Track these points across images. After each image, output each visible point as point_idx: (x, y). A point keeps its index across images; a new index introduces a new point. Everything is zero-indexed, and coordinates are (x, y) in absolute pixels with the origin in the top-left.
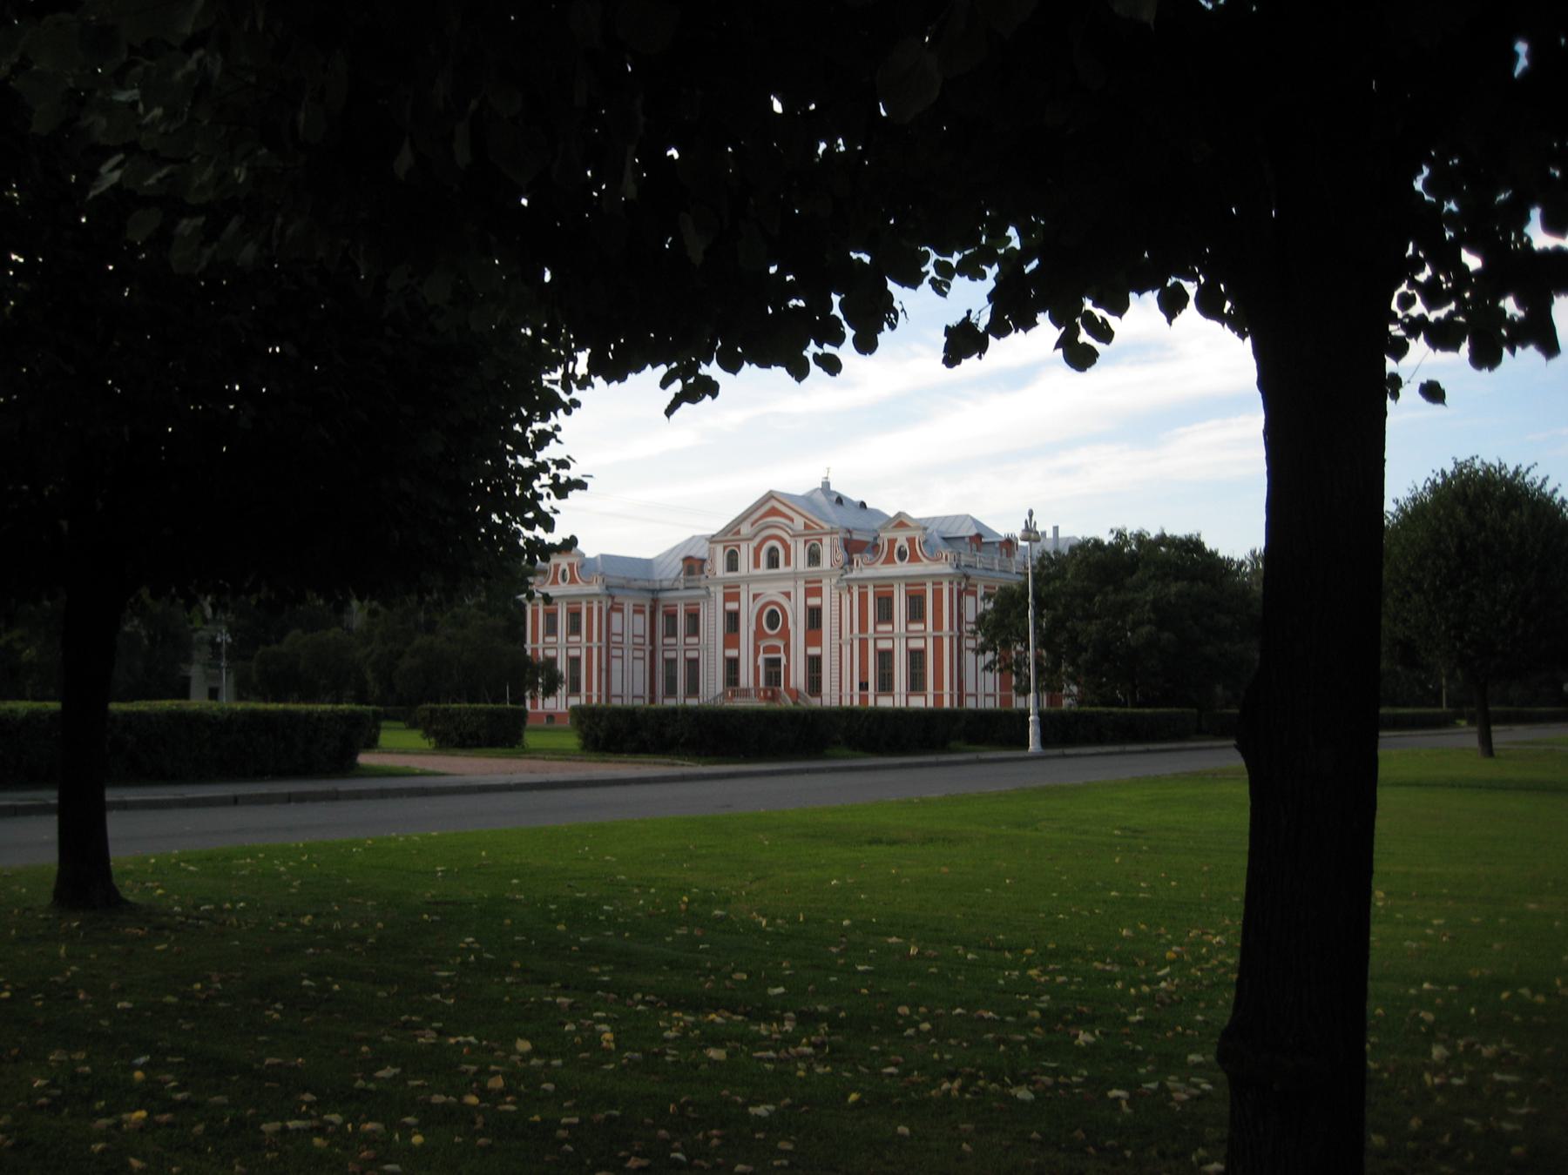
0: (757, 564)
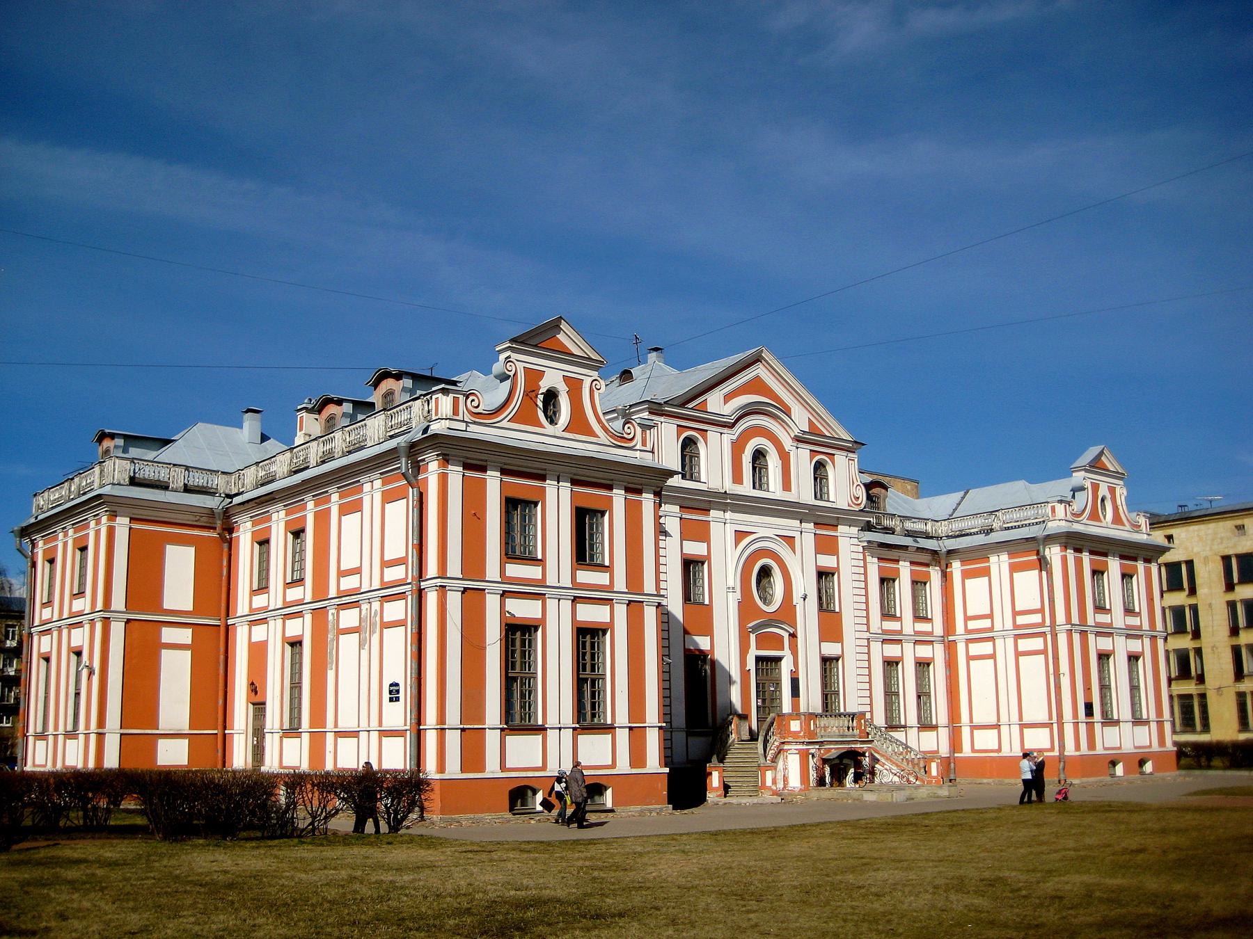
0: (738, 478)
